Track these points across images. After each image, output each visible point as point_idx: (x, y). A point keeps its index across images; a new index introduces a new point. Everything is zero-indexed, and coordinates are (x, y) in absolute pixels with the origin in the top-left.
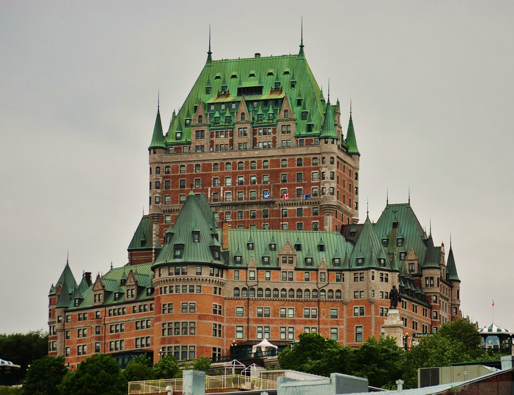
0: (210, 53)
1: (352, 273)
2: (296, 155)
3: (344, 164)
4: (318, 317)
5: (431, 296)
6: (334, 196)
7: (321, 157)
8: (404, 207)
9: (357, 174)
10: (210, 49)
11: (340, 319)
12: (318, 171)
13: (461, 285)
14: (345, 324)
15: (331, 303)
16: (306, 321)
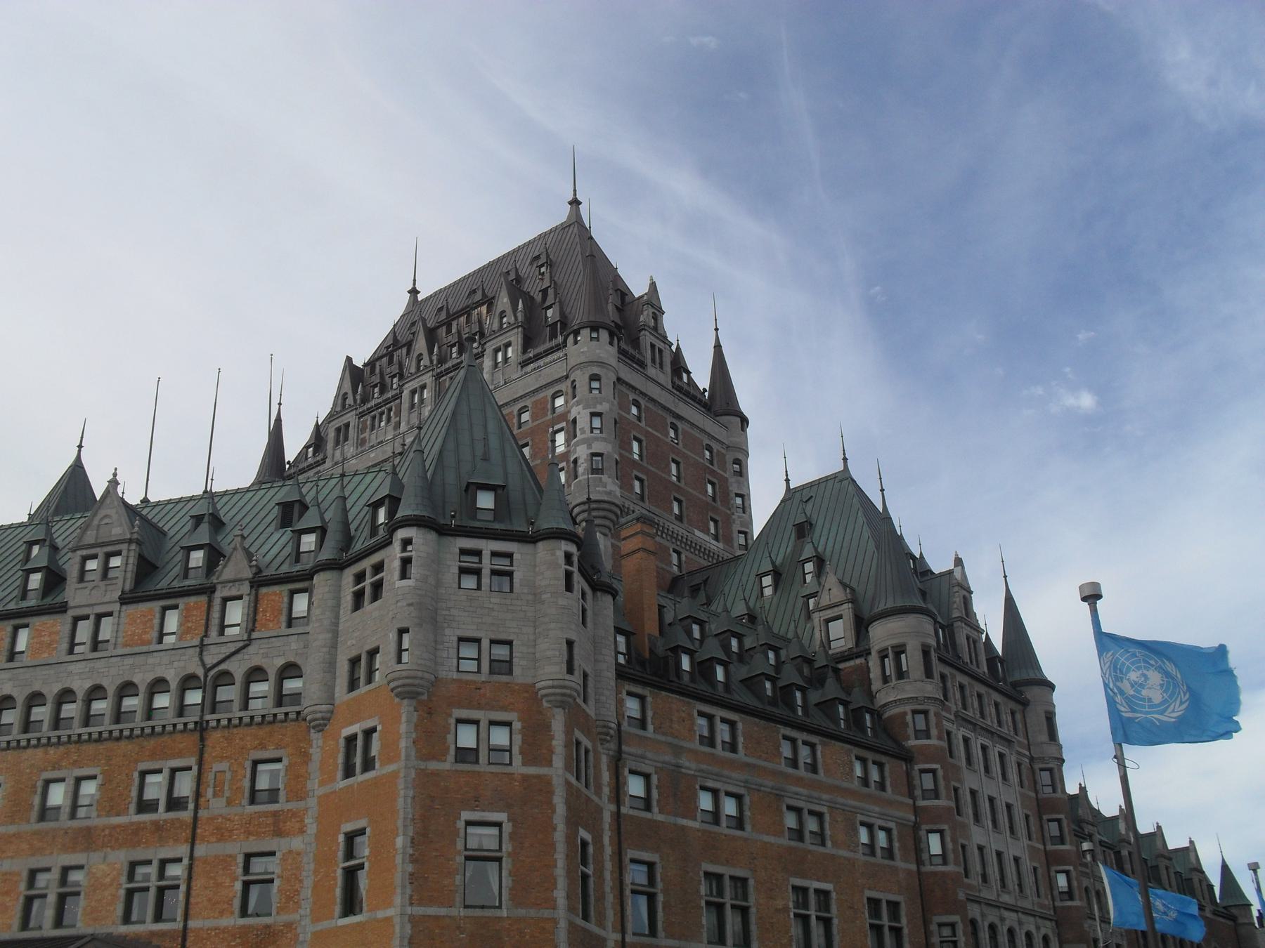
0: (414, 292)
1: (349, 574)
2: (515, 400)
3: (675, 421)
4: (191, 806)
5: (905, 714)
6: (605, 478)
7: (569, 382)
8: (830, 483)
9: (737, 462)
10: (414, 284)
11: (290, 806)
12: (563, 424)
13: (1056, 697)
14: (312, 829)
15: (254, 729)
16: (137, 829)
